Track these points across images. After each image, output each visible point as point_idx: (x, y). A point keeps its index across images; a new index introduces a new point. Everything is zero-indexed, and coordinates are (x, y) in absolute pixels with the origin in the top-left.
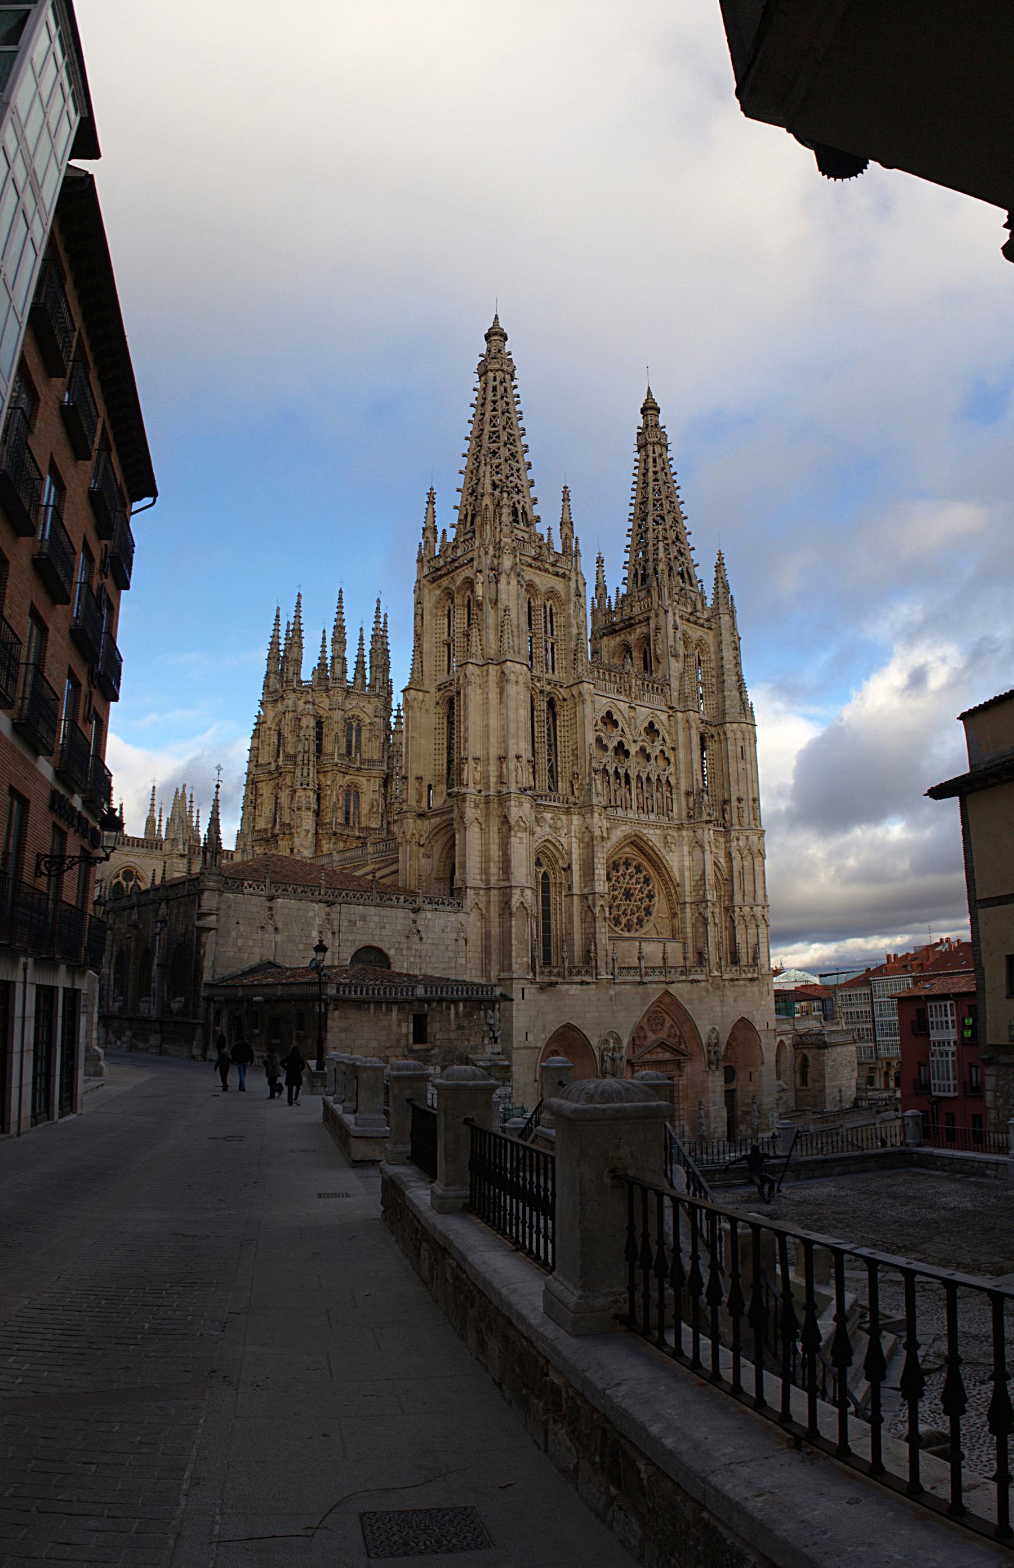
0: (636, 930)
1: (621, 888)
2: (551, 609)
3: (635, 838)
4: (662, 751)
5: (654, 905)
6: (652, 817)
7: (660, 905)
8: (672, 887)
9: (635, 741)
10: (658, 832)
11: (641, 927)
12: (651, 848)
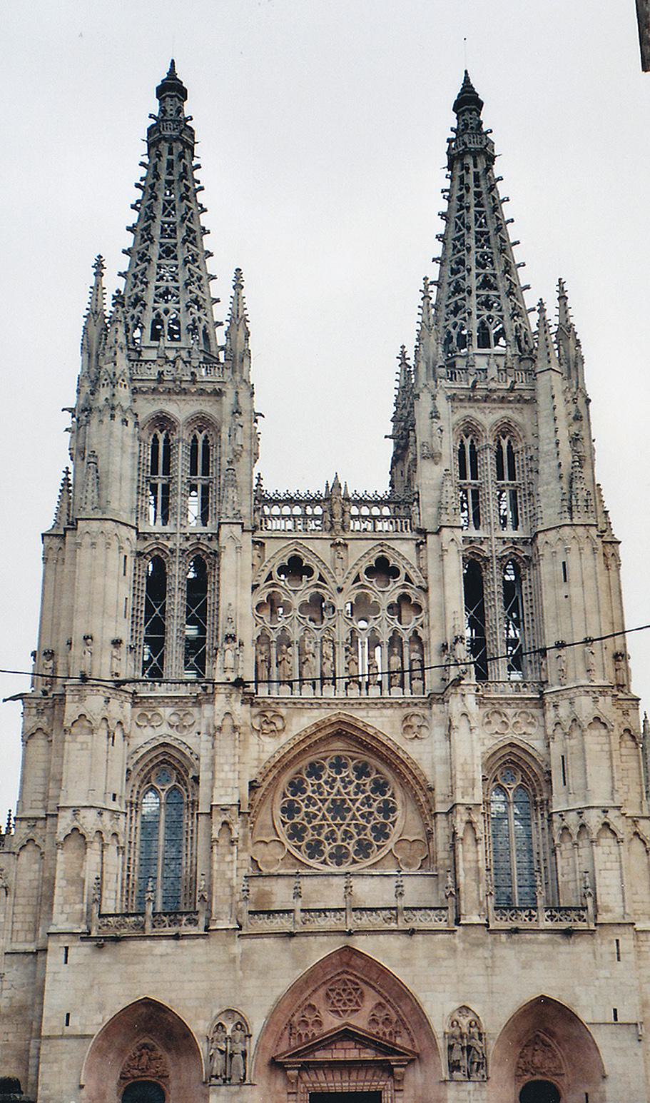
0: (354, 862)
1: (323, 801)
2: (206, 441)
4: (404, 598)
5: (393, 823)
6: (374, 692)
7: (405, 822)
8: (420, 792)
9: (340, 590)
10: (389, 712)
11: (367, 856)
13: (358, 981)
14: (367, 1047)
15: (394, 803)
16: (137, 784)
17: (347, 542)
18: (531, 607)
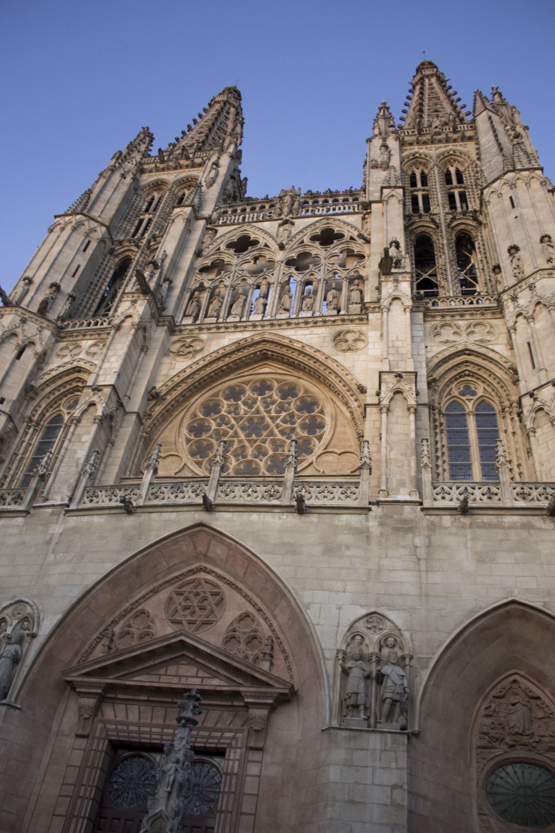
3: (268, 346)
5: (320, 438)
12: (300, 352)
13: (220, 583)
14: (215, 675)
15: (323, 419)
16: (43, 406)
17: (294, 220)
18: (485, 253)
